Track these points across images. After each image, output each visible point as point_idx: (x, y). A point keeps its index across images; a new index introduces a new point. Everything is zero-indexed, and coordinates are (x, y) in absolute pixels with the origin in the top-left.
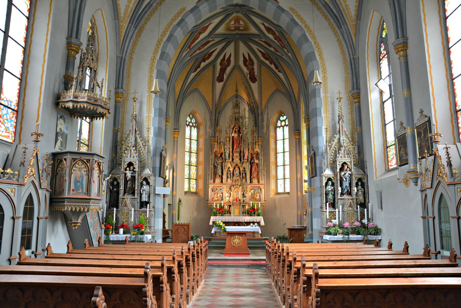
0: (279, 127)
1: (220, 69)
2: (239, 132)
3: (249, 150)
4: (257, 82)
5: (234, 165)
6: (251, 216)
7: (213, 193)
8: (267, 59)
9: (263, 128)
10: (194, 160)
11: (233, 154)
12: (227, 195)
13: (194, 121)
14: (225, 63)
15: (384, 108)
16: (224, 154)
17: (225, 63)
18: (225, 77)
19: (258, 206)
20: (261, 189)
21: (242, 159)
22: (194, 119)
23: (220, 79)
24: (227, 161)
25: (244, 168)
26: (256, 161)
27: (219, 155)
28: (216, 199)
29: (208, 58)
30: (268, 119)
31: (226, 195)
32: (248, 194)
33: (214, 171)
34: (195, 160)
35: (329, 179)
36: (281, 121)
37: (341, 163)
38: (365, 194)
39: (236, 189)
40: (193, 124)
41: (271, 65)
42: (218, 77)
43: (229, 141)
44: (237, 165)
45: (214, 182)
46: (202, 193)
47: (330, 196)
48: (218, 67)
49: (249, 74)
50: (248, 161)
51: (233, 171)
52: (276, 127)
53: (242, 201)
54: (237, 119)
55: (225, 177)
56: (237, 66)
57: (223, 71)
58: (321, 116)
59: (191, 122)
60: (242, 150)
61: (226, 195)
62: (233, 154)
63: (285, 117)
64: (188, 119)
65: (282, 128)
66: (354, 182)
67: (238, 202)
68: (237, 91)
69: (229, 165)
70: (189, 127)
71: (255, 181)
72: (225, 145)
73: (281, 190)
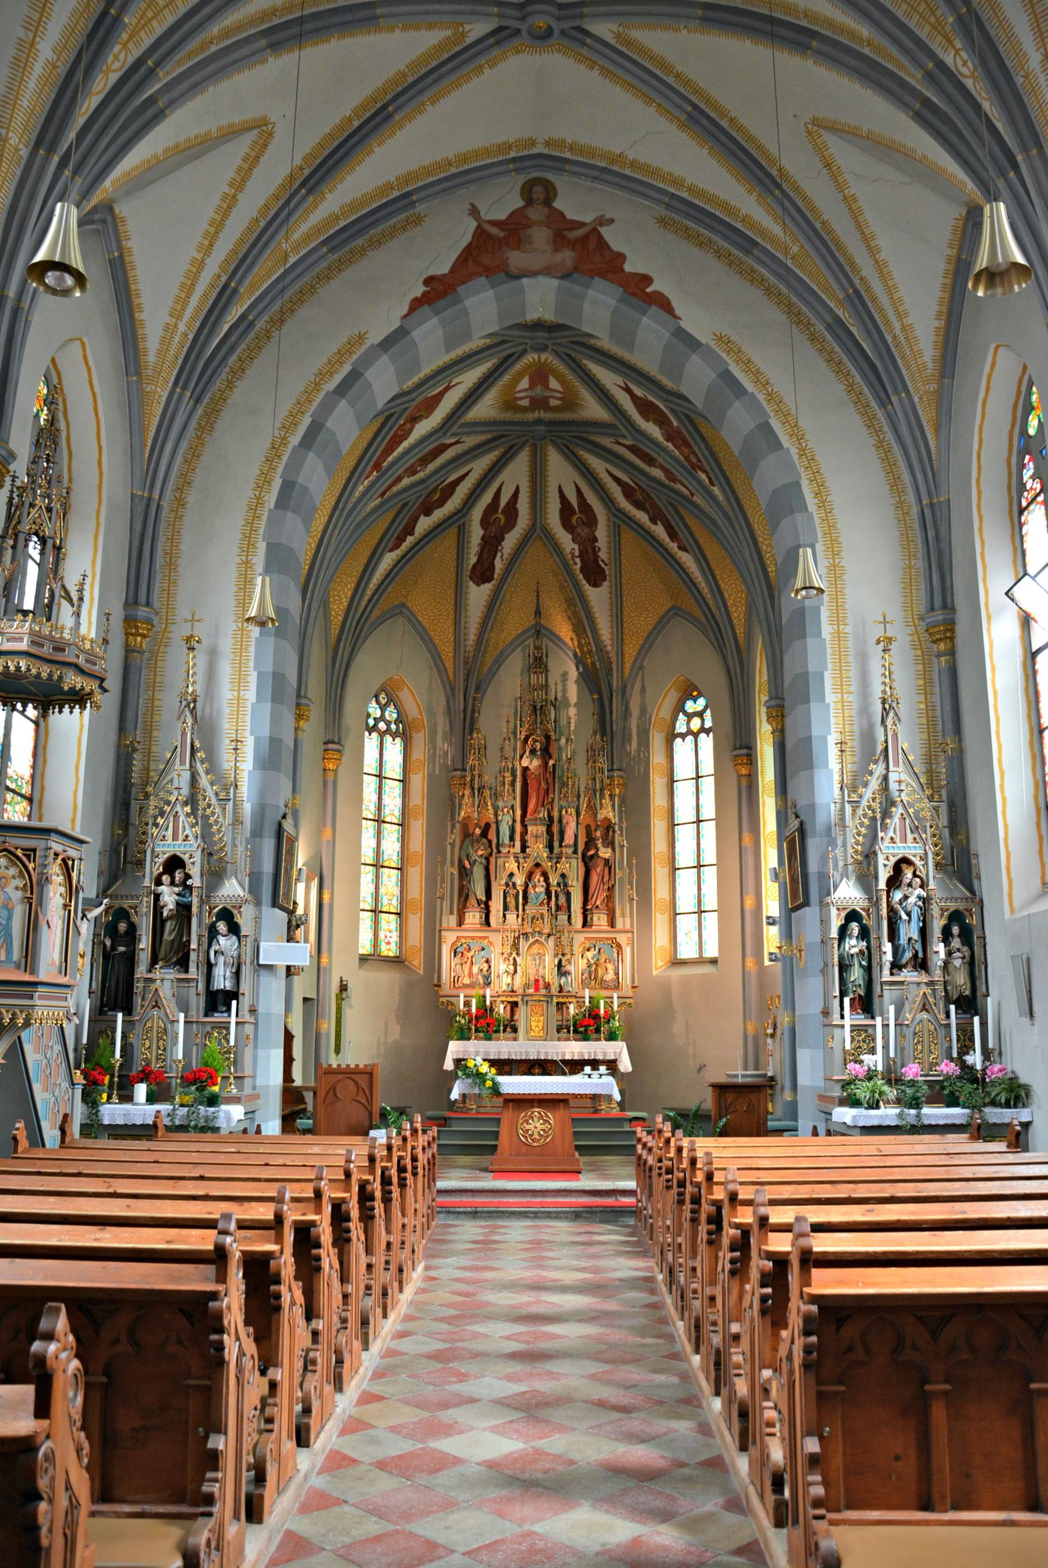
0: (683, 736)
1: (483, 538)
2: (546, 753)
3: (578, 815)
4: (606, 584)
5: (528, 865)
6: (585, 1039)
7: (458, 960)
8: (639, 505)
9: (626, 739)
10: (391, 847)
11: (524, 826)
12: (503, 967)
13: (391, 714)
14: (499, 520)
15: (1035, 673)
16: (493, 827)
17: (499, 520)
18: (499, 564)
19: (609, 1004)
20: (619, 946)
21: (556, 844)
22: (391, 708)
23: (482, 573)
24: (504, 850)
25: (563, 876)
26: (605, 853)
27: (478, 831)
28: (467, 981)
29: (441, 503)
30: (643, 710)
31: (501, 966)
32: (578, 966)
33: (461, 888)
34: (397, 846)
35: (852, 916)
36: (690, 716)
37: (893, 860)
38: (975, 967)
39: (535, 949)
40: (388, 723)
41: (653, 527)
42: (474, 566)
43: (513, 783)
44: (538, 865)
45: (460, 923)
46: (417, 962)
47: (856, 974)
48: (476, 534)
49: (581, 556)
50: (575, 852)
51: (527, 886)
52: (671, 737)
53: (554, 989)
54: (539, 709)
55: (496, 905)
56: (538, 530)
57: (491, 544)
58: (823, 700)
59: (382, 718)
60: (556, 814)
61: (501, 966)
62: (524, 826)
63: (701, 702)
64: (374, 710)
65: (690, 739)
66: (937, 925)
67: (543, 991)
68: (538, 613)
69: (512, 865)
70: (375, 735)
71: (600, 920)
72: (496, 796)
73: (687, 950)
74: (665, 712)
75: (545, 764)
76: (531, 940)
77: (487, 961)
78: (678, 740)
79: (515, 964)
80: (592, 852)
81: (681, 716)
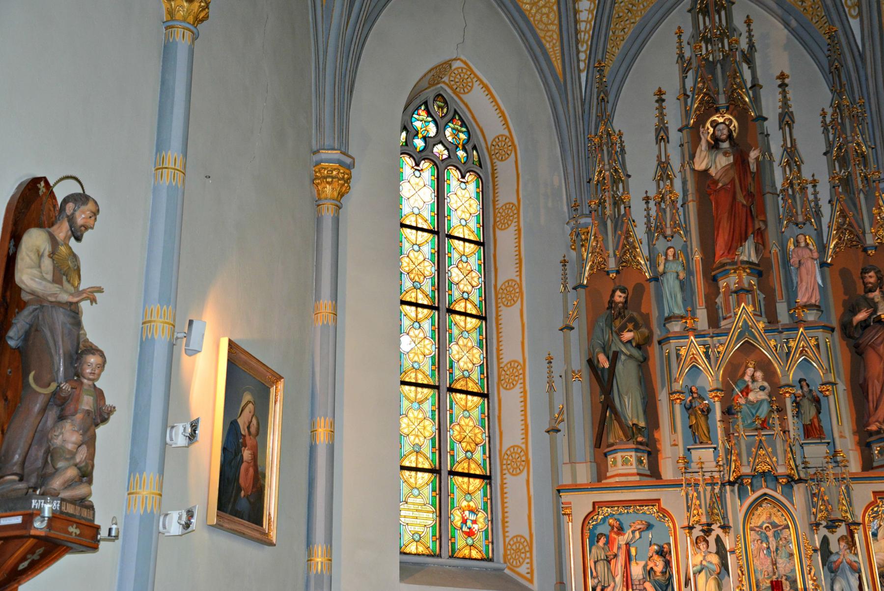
5: (728, 347)
7: (597, 552)
11: (712, 281)
12: (694, 559)
34: (477, 355)
39: (761, 517)
45: (601, 474)
59: (439, 138)
75: (741, 161)
76: (753, 497)
77: (662, 553)
79: (721, 551)
80: (861, 316)
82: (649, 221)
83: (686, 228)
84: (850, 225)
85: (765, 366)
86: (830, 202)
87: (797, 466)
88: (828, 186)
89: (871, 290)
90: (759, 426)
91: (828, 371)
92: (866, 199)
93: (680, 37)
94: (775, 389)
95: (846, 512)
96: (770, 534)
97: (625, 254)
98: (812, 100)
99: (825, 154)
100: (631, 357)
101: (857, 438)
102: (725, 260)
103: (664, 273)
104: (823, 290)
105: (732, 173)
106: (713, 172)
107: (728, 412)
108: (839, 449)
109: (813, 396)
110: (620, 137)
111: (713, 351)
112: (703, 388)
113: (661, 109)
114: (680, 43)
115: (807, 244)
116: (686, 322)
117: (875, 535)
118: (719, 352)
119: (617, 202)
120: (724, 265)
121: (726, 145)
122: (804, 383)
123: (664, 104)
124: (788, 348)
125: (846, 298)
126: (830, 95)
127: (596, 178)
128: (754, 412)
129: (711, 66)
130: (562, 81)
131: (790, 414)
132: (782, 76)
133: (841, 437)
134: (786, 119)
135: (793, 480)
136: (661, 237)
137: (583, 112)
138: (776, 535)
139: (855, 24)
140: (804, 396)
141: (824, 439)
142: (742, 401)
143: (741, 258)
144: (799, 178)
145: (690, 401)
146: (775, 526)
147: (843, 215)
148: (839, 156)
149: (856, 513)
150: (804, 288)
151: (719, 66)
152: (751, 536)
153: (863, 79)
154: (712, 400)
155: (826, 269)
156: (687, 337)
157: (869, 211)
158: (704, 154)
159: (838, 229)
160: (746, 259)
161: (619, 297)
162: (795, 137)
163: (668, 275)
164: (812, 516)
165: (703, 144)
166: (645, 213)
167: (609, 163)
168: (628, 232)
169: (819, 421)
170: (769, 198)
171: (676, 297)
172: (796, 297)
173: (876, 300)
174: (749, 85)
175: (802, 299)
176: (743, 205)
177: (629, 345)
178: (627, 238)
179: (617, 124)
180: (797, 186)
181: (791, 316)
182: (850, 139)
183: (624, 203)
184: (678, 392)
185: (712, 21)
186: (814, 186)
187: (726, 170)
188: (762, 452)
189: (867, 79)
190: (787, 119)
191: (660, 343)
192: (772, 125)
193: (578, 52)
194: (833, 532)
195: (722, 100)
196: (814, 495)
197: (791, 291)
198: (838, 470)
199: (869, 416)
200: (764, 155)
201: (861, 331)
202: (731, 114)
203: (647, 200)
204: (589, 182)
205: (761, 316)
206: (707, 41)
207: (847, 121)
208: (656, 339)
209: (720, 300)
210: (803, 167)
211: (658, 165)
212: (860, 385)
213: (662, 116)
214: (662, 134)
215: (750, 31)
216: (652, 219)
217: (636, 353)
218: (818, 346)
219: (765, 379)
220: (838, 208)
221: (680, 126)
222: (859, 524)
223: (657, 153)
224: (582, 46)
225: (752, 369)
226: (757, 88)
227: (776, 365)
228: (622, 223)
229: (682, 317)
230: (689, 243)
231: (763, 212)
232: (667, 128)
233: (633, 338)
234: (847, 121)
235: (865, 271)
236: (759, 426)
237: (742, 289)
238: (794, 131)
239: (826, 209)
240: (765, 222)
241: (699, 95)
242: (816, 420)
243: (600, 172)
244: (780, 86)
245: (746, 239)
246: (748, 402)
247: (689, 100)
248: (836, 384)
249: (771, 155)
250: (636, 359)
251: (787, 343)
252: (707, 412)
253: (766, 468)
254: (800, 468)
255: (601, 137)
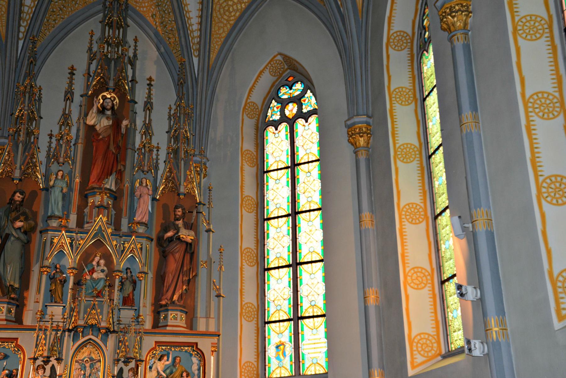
0: (276, 124)
5: (86, 241)
11: (84, 197)
36: (284, 104)
39: (84, 354)
52: (262, 125)
63: (299, 87)
65: (284, 127)
71: (176, 319)
74: (257, 98)
75: (117, 125)
76: (82, 340)
78: (271, 129)
80: (170, 234)
81: (274, 103)
82: (49, 150)
83: (73, 160)
84: (173, 178)
85: (107, 257)
86: (165, 162)
87: (113, 323)
88: (166, 152)
89: (178, 220)
90: (95, 295)
91: (144, 265)
92: (185, 164)
93: (92, 36)
94: (111, 271)
95: (137, 353)
96: (88, 365)
97: (28, 169)
98: (165, 98)
99: (167, 132)
100: (18, 239)
101: (153, 308)
102: (95, 185)
103: (53, 186)
104: (151, 215)
105: (110, 132)
106: (98, 127)
107: (78, 283)
108: (141, 314)
109: (133, 280)
110: (40, 91)
111: (76, 243)
112: (64, 266)
113: (71, 79)
114: (91, 41)
115: (147, 185)
116: (62, 221)
117: (151, 368)
118: (79, 244)
119: (29, 134)
120: (93, 188)
121: (109, 113)
122: (129, 271)
123: (74, 77)
124: (123, 247)
125: (163, 222)
126: (176, 98)
127: (17, 114)
128: (94, 285)
129: (108, 61)
130: (4, 41)
131: (116, 289)
132: (150, 79)
133: (144, 306)
134: (148, 106)
135: (110, 331)
136: (56, 162)
137: (16, 67)
138: (92, 366)
139: (195, 60)
140: (127, 279)
141: (134, 306)
142: (88, 277)
143: (106, 186)
144: (150, 143)
145: (54, 274)
146: (92, 359)
147: (171, 171)
148: (175, 136)
149: (143, 354)
150: (140, 212)
151: (113, 62)
152: (76, 366)
153: (195, 93)
154: (69, 275)
155: (155, 202)
156: (61, 231)
157: (185, 172)
158: (94, 115)
159: (166, 179)
160: (108, 187)
161: (18, 197)
162: (152, 118)
163: (56, 188)
164: (116, 355)
165: (95, 109)
166: (48, 144)
167: (28, 106)
168: (33, 154)
169: (133, 295)
170: (129, 151)
171: (58, 204)
172: (134, 216)
173: (180, 226)
174: (130, 79)
175: (137, 218)
176: (113, 153)
177: (18, 231)
178: (31, 159)
179: (39, 82)
180: (148, 148)
181: (129, 227)
182: (182, 127)
183: (34, 135)
184: (47, 267)
185: (114, 33)
186: (158, 150)
187: (106, 128)
188: (94, 312)
189: (197, 94)
190: (149, 106)
191: (41, 232)
192: (139, 107)
193: (20, 25)
194: (126, 365)
195: (111, 84)
196: (120, 341)
197: (132, 212)
198: (138, 327)
199: (163, 296)
200: (131, 124)
201: (168, 243)
202: (116, 94)
203: (51, 136)
204: (11, 115)
205: (111, 225)
206: (109, 45)
207: (182, 116)
208: (39, 229)
209: (87, 210)
210: (153, 137)
211: (63, 115)
212: (161, 276)
213: (71, 84)
214: (69, 95)
215: (136, 46)
216: (52, 149)
217: (22, 237)
218: (141, 249)
219: (105, 265)
220: (168, 167)
221: (82, 93)
222: (143, 361)
223: (64, 107)
224: (23, 22)
225: (99, 258)
226: (134, 82)
227: (114, 257)
228: (30, 146)
229: (60, 218)
230: (73, 170)
231: (124, 160)
232: (73, 93)
233: (23, 227)
234: (182, 116)
235: (176, 207)
236: (95, 295)
237: (102, 206)
238: (152, 114)
239: (162, 166)
240: (124, 166)
241: (97, 77)
242: (131, 295)
243: (21, 110)
244: (148, 85)
245: (111, 174)
246: (92, 279)
247: (91, 79)
248: (147, 274)
249: (135, 125)
250: (22, 241)
251: (124, 244)
252: (64, 282)
253: (94, 322)
254: (115, 324)
255: (26, 87)
